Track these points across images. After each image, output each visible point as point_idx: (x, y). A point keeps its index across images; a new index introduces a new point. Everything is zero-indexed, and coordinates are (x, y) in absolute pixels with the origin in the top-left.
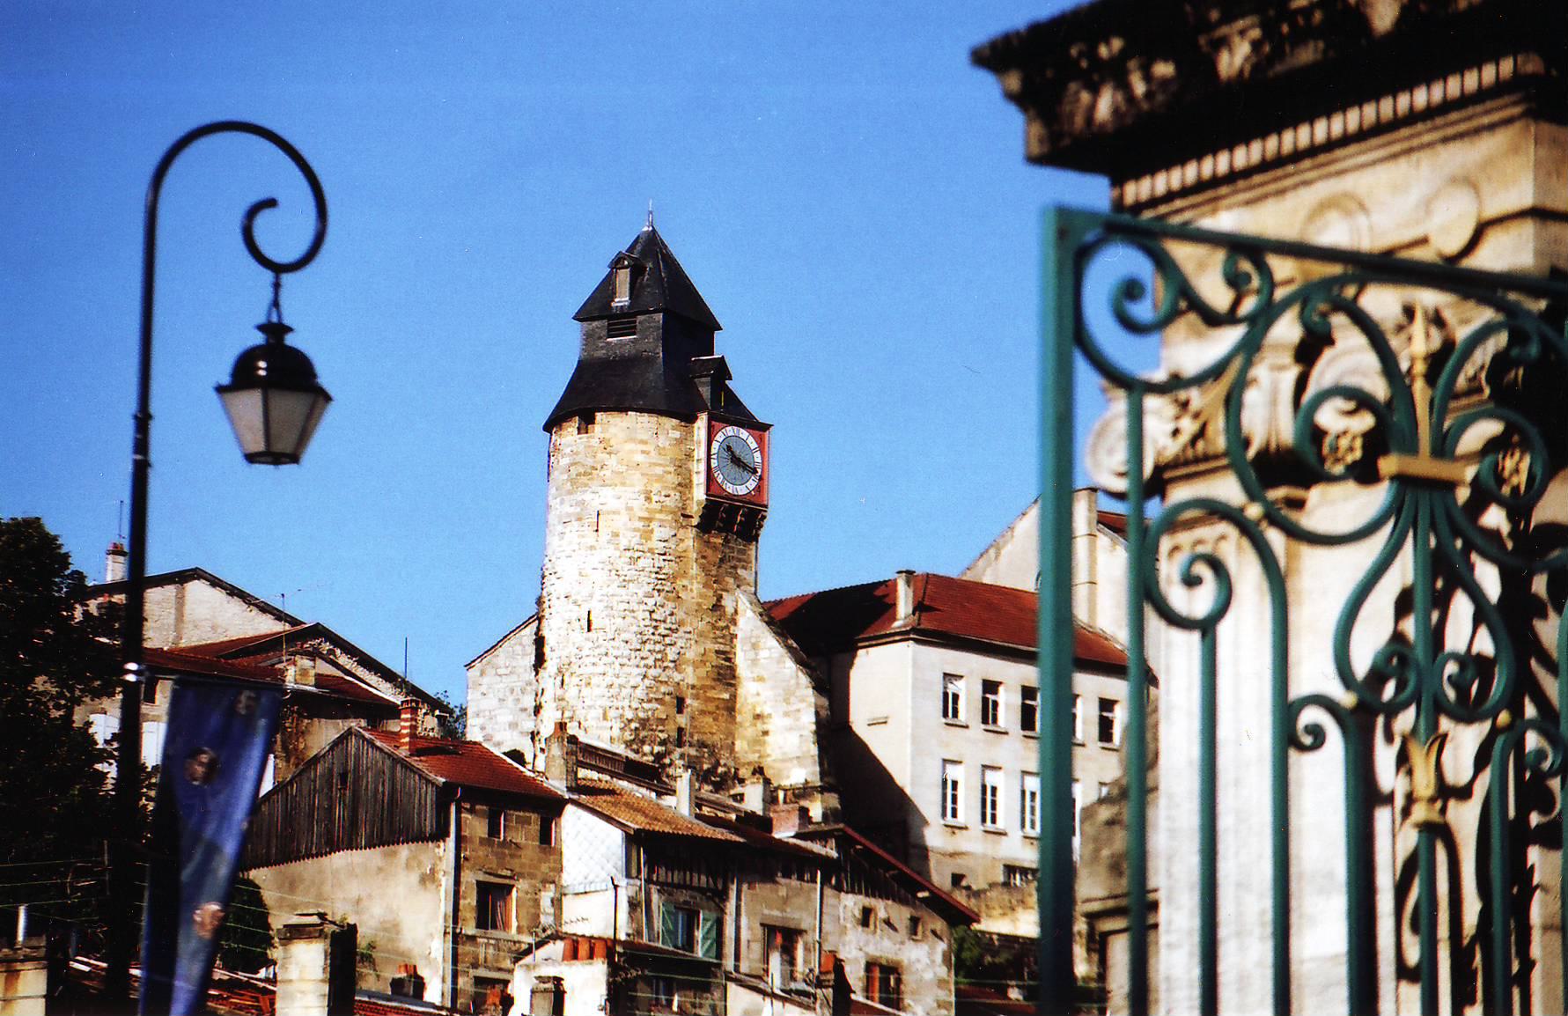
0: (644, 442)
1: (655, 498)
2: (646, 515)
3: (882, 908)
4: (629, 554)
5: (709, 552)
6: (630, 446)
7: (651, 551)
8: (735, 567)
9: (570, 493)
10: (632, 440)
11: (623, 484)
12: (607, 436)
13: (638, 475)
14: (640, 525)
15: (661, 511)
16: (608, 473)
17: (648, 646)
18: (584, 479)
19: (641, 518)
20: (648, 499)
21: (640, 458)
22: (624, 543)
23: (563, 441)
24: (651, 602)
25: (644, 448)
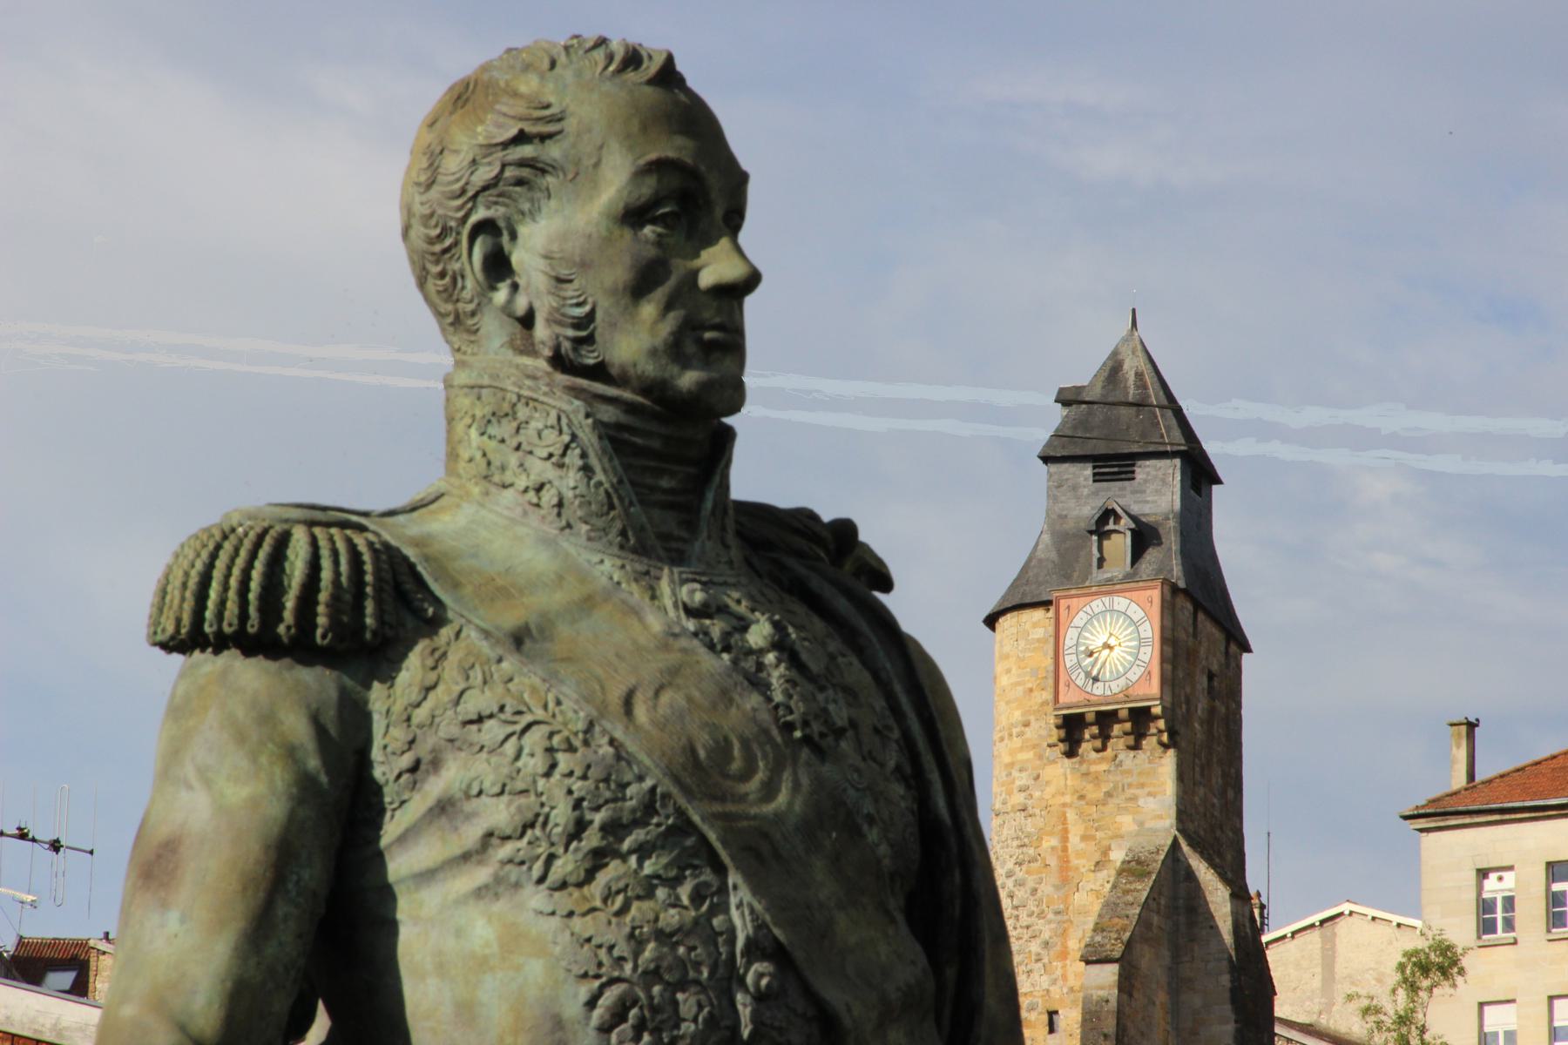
8: (1134, 799)
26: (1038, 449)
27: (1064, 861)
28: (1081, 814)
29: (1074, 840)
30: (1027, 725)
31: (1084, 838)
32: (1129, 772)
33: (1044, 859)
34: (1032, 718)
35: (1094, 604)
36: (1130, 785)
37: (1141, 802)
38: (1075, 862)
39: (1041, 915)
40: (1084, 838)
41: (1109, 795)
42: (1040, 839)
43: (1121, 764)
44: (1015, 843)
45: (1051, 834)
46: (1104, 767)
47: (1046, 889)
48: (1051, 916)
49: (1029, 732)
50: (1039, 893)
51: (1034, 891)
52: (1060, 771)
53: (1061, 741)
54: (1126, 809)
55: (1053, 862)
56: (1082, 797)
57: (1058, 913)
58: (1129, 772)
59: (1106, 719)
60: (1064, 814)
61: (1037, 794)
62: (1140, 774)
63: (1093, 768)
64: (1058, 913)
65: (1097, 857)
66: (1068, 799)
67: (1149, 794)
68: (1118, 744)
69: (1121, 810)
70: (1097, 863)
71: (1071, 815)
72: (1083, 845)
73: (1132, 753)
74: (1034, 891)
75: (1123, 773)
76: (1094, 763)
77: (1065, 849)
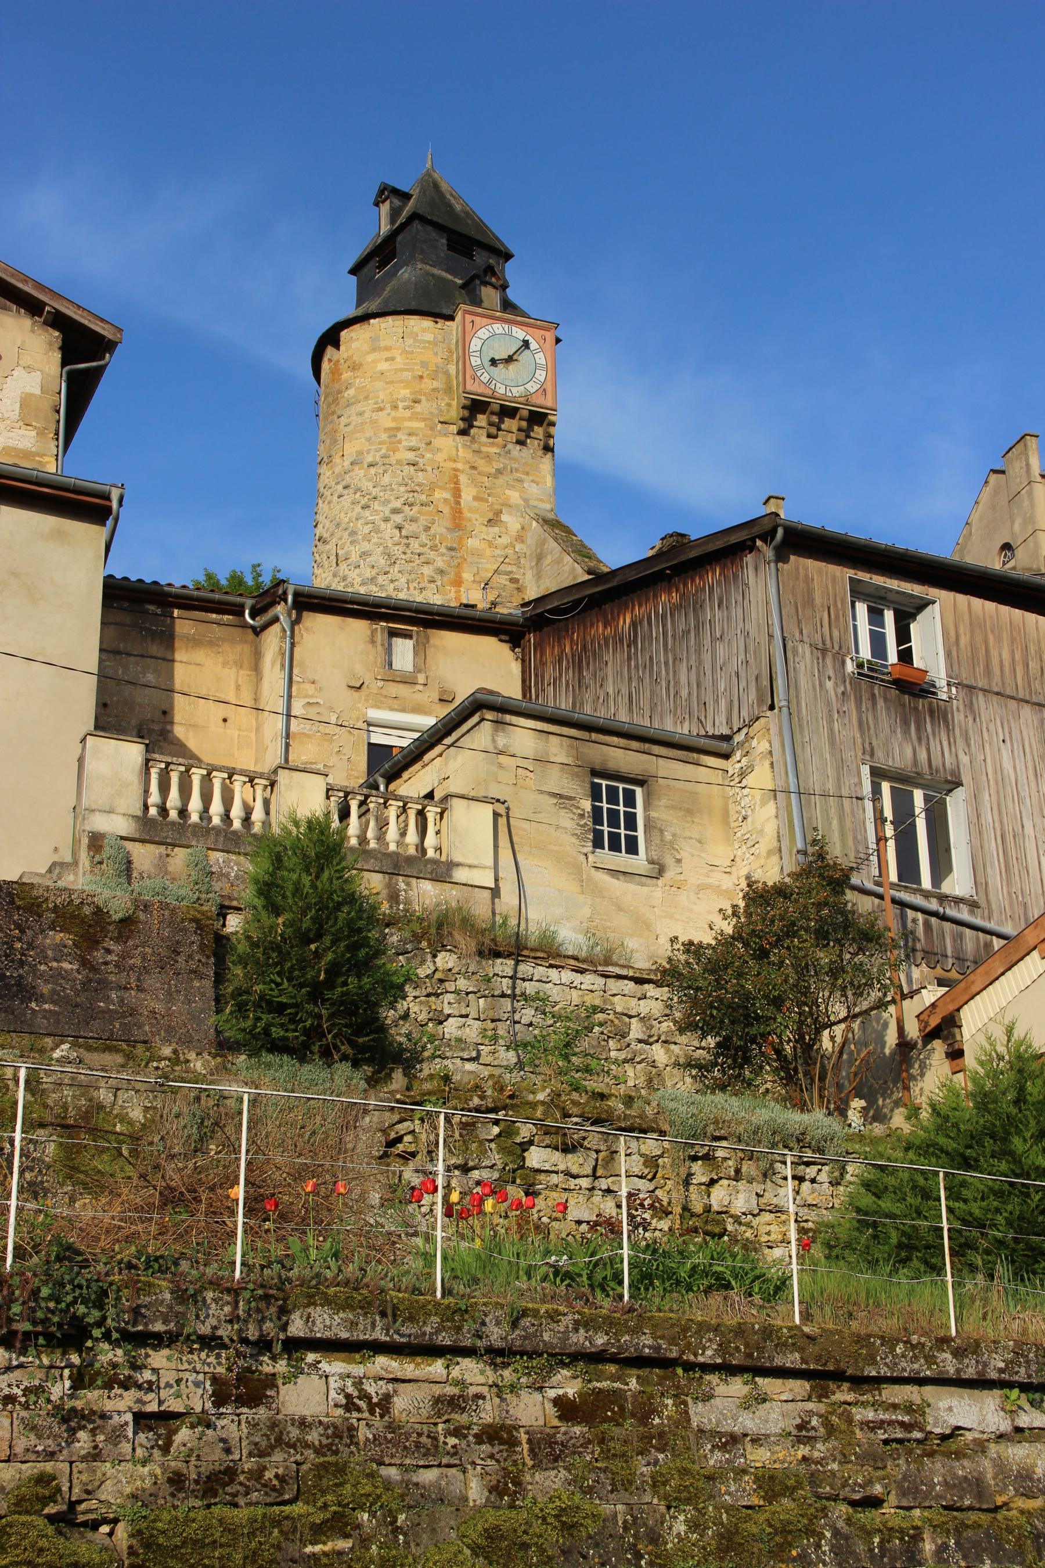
0: (388, 349)
1: (401, 405)
2: (393, 425)
4: (373, 471)
5: (480, 463)
6: (370, 358)
7: (399, 462)
10: (374, 350)
12: (350, 353)
15: (410, 419)
16: (351, 392)
17: (397, 568)
19: (386, 430)
20: (395, 407)
21: (383, 366)
22: (369, 459)
24: (398, 519)
25: (389, 354)
27: (457, 511)
30: (416, 402)
31: (476, 498)
32: (515, 460)
33: (437, 506)
34: (423, 398)
35: (495, 326)
36: (517, 470)
38: (467, 514)
39: (434, 548)
41: (499, 472)
42: (432, 490)
43: (509, 452)
44: (403, 489)
45: (442, 488)
46: (494, 450)
47: (440, 529)
48: (443, 550)
49: (418, 408)
50: (432, 531)
51: (427, 529)
52: (449, 445)
53: (462, 419)
54: (514, 487)
55: (446, 510)
56: (474, 468)
57: (451, 549)
58: (515, 460)
59: (508, 412)
60: (456, 476)
63: (484, 449)
64: (451, 549)
65: (490, 516)
66: (459, 466)
69: (510, 486)
70: (490, 521)
71: (463, 479)
72: (476, 504)
73: (518, 447)
74: (427, 529)
75: (511, 459)
76: (485, 445)
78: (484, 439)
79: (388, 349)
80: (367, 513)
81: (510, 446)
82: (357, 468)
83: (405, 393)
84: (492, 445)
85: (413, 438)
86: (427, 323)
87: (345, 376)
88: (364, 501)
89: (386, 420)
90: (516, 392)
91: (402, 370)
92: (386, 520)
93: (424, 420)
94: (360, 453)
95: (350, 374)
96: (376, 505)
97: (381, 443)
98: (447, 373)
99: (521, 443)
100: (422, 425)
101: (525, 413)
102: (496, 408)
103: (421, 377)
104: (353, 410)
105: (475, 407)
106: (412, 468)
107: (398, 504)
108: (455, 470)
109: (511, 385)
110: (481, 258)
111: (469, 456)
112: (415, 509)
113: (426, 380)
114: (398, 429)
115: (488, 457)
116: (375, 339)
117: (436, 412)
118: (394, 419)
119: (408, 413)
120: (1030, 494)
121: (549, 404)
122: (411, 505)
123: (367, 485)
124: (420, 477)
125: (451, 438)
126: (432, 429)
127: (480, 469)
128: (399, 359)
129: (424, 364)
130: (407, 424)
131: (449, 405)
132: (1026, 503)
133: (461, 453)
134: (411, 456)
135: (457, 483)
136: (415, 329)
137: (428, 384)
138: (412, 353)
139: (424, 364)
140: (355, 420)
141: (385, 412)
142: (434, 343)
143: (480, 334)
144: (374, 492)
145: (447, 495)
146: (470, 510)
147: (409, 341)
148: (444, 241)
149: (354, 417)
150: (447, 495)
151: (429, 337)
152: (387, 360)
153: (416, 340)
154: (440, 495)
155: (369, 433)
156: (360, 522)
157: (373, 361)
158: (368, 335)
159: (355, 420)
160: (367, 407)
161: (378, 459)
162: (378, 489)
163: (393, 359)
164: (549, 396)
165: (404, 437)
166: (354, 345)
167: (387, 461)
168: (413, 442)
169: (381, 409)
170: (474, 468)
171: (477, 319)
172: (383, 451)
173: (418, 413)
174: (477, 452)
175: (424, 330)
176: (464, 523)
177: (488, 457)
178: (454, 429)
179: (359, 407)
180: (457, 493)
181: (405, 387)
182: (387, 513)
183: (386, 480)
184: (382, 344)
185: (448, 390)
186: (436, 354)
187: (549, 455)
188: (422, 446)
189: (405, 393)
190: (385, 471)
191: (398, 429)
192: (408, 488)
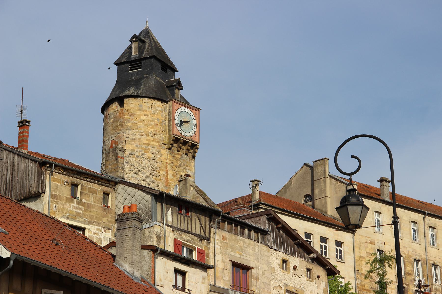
0: (146, 111)
1: (150, 135)
2: (147, 142)
3: (294, 261)
4: (139, 159)
5: (174, 161)
6: (138, 113)
7: (149, 158)
8: (185, 169)
9: (113, 134)
10: (140, 110)
11: (136, 129)
12: (129, 108)
13: (143, 125)
14: (143, 146)
15: (153, 141)
16: (130, 124)
18: (119, 127)
19: (144, 144)
20: (148, 135)
21: (144, 118)
22: (137, 154)
23: (110, 112)
24: (148, 180)
25: (146, 113)
26: (115, 61)
27: (167, 180)
28: (172, 167)
29: (170, 175)
31: (173, 175)
33: (161, 177)
34: (158, 133)
37: (187, 171)
38: (170, 181)
40: (173, 175)
41: (180, 165)
43: (183, 158)
44: (150, 169)
45: (163, 170)
49: (156, 137)
52: (165, 153)
55: (164, 179)
56: (172, 163)
59: (185, 143)
60: (167, 166)
61: (159, 157)
62: (187, 162)
63: (176, 156)
66: (168, 162)
67: (189, 169)
68: (182, 152)
71: (169, 167)
72: (172, 177)
73: (185, 156)
75: (183, 160)
77: (167, 176)
78: (176, 152)
79: (146, 111)
80: (136, 176)
81: (183, 155)
82: (132, 156)
83: (151, 130)
84: (178, 154)
85: (154, 149)
86: (159, 103)
87: (126, 117)
88: (135, 171)
89: (144, 139)
90: (188, 135)
91: (151, 121)
92: (144, 180)
93: (158, 142)
94: (133, 150)
95: (128, 117)
96: (140, 173)
97: (142, 149)
98: (165, 124)
99: (186, 154)
100: (157, 144)
101: (190, 144)
102: (182, 141)
103: (157, 125)
104: (131, 132)
105: (176, 140)
106: (153, 161)
107: (148, 174)
108: (167, 163)
109: (186, 132)
110: (169, 72)
111: (171, 158)
112: (154, 177)
113: (158, 126)
114: (149, 144)
115: (177, 159)
116: (140, 106)
117: (161, 139)
118: (147, 140)
119: (152, 139)
120: (325, 182)
121: (197, 141)
122: (153, 176)
123: (136, 164)
124: (156, 165)
125: (166, 151)
126: (160, 146)
127: (174, 163)
128: (149, 116)
129: (158, 120)
130: (152, 143)
131: (165, 137)
132: (322, 184)
133: (168, 157)
134: (153, 156)
135: (167, 168)
136: (156, 105)
137: (159, 128)
138: (154, 114)
139: (158, 120)
140: (131, 137)
141: (144, 137)
142: (161, 112)
143: (178, 111)
144: (139, 168)
145: (164, 173)
146: (171, 180)
147: (154, 110)
148: (160, 66)
149: (131, 135)
150: (164, 173)
151: (160, 109)
152: (145, 115)
153: (156, 110)
154: (163, 173)
155: (137, 143)
156: (133, 178)
157: (140, 115)
158: (137, 103)
159: (131, 137)
160: (137, 133)
161: (141, 155)
162: (141, 167)
163: (147, 116)
164: (197, 138)
165: (151, 148)
166: (131, 106)
167: (144, 156)
168: (154, 150)
169: (143, 135)
170: (172, 163)
171: (177, 105)
172: (143, 152)
173: (156, 139)
174: (174, 157)
175: (158, 106)
176: (169, 184)
177: (177, 159)
178: (167, 147)
179: (134, 132)
180: (167, 173)
181: (152, 128)
182: (144, 177)
183: (144, 164)
184: (144, 109)
185: (165, 131)
186: (162, 116)
187: (194, 159)
188: (157, 152)
189: (151, 130)
190: (144, 161)
191: (149, 144)
192: (152, 169)
